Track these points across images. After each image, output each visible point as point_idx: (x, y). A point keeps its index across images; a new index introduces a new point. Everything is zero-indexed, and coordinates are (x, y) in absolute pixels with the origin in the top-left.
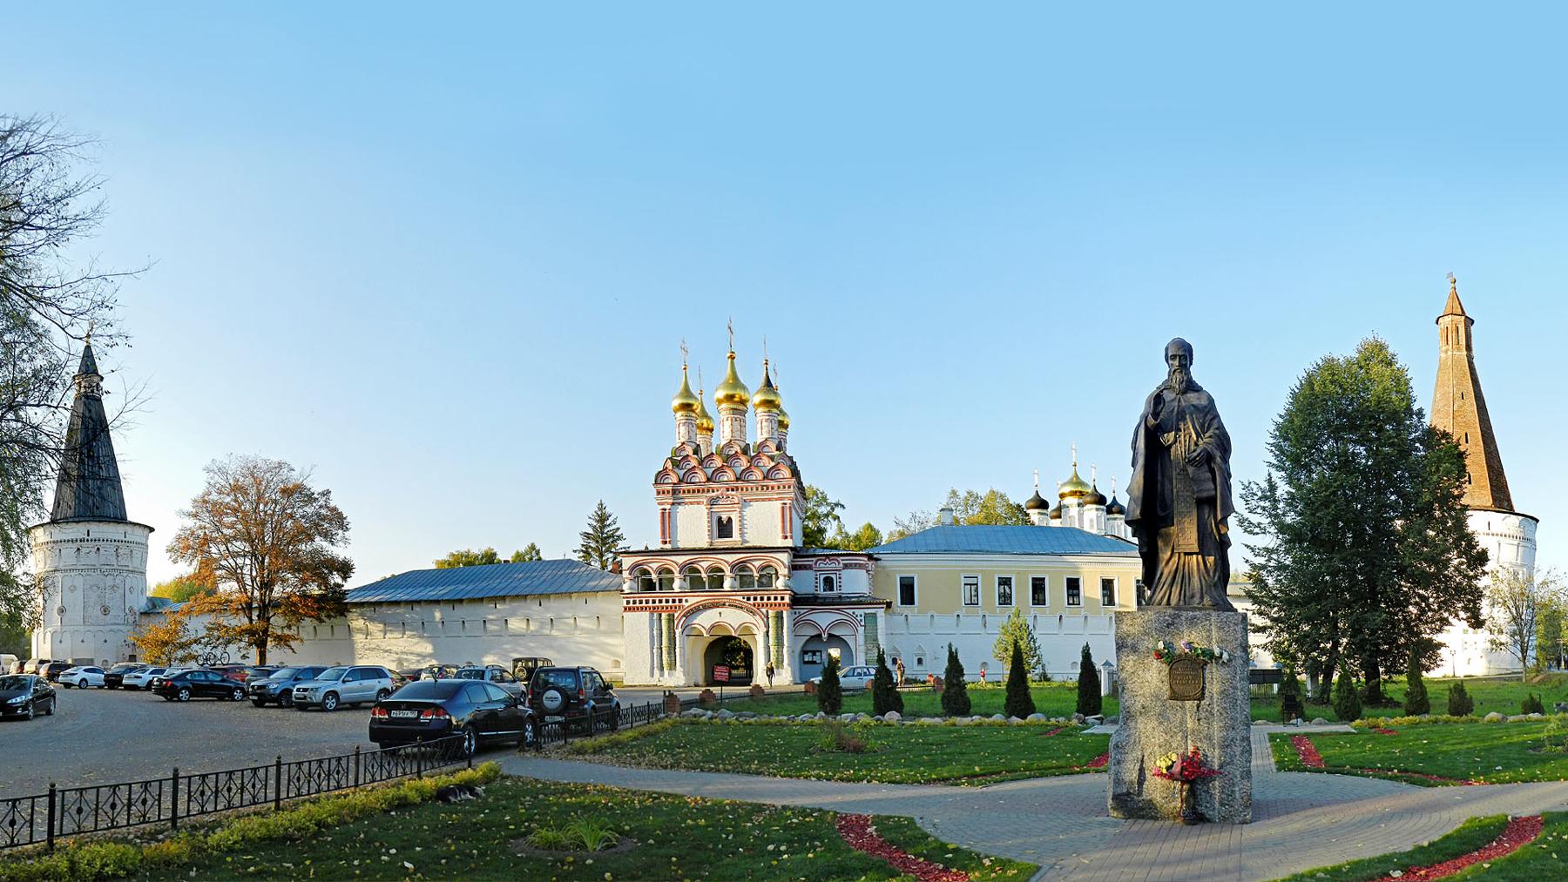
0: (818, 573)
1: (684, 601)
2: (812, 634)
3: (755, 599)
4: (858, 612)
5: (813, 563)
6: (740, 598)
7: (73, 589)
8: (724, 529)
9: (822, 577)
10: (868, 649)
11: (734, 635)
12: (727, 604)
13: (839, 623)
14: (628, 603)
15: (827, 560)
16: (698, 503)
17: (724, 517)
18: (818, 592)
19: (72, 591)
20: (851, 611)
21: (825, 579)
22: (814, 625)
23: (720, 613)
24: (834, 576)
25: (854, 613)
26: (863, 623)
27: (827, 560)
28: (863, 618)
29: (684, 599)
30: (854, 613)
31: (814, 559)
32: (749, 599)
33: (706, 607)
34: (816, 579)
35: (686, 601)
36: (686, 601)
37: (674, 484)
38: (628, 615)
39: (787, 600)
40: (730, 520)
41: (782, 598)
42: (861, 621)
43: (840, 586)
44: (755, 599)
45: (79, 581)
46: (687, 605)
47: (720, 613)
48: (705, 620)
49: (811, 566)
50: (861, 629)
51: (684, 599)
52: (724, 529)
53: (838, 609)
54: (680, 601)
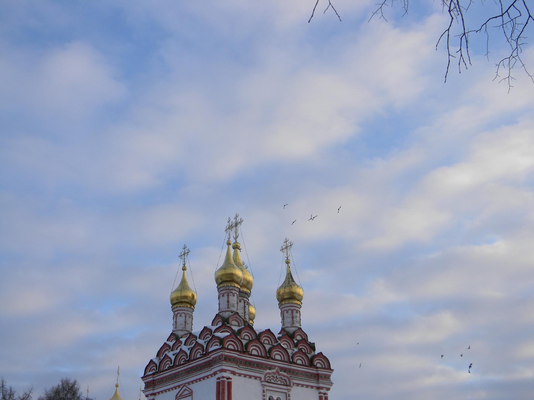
16: (256, 378)
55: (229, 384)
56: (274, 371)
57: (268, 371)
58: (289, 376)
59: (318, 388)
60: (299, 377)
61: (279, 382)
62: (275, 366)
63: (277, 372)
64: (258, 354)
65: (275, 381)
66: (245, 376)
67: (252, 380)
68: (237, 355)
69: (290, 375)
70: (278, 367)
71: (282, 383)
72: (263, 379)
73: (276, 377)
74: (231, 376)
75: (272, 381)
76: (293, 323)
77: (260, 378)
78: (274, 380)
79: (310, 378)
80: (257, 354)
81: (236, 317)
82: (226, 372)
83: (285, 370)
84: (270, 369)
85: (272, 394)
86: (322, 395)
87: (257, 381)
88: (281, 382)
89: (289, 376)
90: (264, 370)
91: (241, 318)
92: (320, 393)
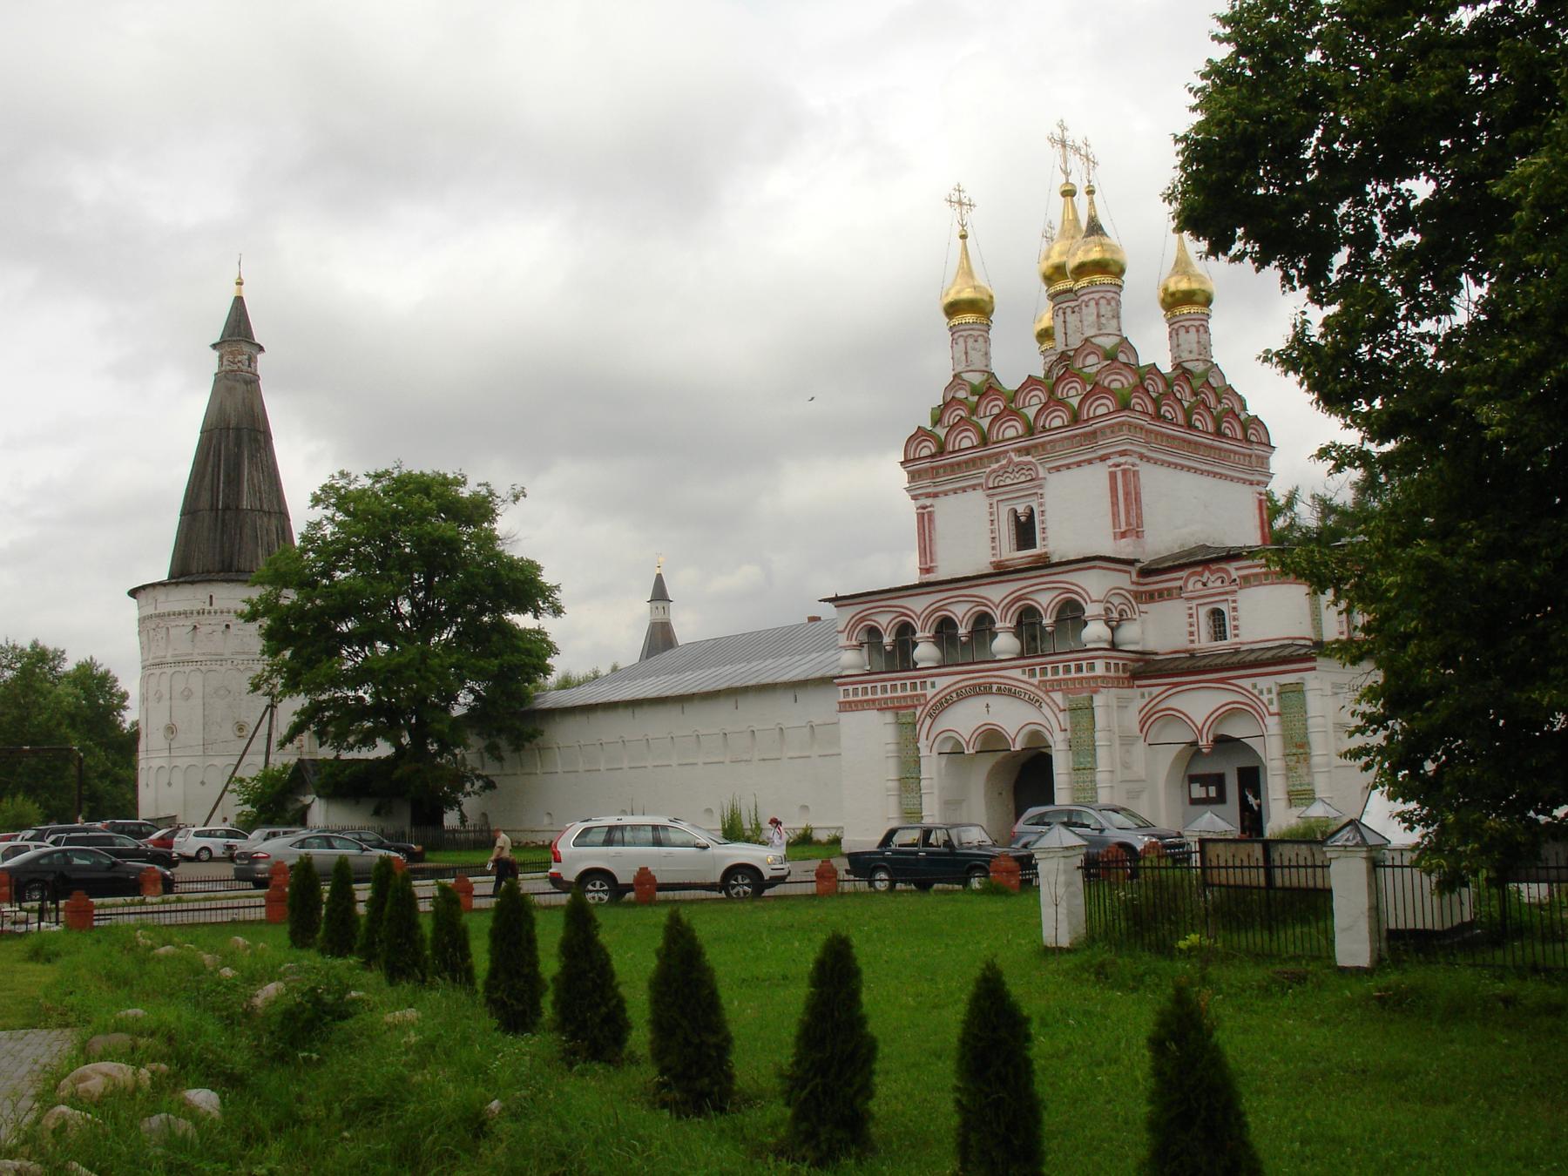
0: (1195, 603)
1: (928, 684)
3: (1044, 672)
4: (1264, 683)
6: (1017, 673)
7: (188, 695)
8: (1025, 531)
9: (1203, 611)
10: (1288, 768)
12: (995, 687)
13: (1232, 713)
15: (1207, 574)
16: (974, 487)
17: (1021, 509)
18: (1196, 645)
19: (187, 698)
20: (1246, 683)
22: (1176, 717)
23: (987, 706)
24: (1223, 607)
25: (1255, 686)
28: (1274, 696)
30: (1255, 686)
33: (962, 695)
34: (1191, 616)
36: (933, 685)
41: (1092, 667)
44: (1044, 672)
45: (196, 682)
46: (930, 692)
47: (987, 706)
48: (966, 720)
51: (929, 680)
52: (1025, 531)
55: (930, 514)
56: (1004, 462)
59: (1103, 459)
61: (1023, 479)
62: (1007, 452)
66: (955, 491)
67: (971, 494)
70: (1013, 450)
71: (1029, 478)
74: (928, 502)
75: (1009, 481)
77: (980, 485)
80: (970, 445)
83: (1027, 451)
84: (997, 461)
87: (980, 493)
89: (1033, 460)
92: (1110, 467)
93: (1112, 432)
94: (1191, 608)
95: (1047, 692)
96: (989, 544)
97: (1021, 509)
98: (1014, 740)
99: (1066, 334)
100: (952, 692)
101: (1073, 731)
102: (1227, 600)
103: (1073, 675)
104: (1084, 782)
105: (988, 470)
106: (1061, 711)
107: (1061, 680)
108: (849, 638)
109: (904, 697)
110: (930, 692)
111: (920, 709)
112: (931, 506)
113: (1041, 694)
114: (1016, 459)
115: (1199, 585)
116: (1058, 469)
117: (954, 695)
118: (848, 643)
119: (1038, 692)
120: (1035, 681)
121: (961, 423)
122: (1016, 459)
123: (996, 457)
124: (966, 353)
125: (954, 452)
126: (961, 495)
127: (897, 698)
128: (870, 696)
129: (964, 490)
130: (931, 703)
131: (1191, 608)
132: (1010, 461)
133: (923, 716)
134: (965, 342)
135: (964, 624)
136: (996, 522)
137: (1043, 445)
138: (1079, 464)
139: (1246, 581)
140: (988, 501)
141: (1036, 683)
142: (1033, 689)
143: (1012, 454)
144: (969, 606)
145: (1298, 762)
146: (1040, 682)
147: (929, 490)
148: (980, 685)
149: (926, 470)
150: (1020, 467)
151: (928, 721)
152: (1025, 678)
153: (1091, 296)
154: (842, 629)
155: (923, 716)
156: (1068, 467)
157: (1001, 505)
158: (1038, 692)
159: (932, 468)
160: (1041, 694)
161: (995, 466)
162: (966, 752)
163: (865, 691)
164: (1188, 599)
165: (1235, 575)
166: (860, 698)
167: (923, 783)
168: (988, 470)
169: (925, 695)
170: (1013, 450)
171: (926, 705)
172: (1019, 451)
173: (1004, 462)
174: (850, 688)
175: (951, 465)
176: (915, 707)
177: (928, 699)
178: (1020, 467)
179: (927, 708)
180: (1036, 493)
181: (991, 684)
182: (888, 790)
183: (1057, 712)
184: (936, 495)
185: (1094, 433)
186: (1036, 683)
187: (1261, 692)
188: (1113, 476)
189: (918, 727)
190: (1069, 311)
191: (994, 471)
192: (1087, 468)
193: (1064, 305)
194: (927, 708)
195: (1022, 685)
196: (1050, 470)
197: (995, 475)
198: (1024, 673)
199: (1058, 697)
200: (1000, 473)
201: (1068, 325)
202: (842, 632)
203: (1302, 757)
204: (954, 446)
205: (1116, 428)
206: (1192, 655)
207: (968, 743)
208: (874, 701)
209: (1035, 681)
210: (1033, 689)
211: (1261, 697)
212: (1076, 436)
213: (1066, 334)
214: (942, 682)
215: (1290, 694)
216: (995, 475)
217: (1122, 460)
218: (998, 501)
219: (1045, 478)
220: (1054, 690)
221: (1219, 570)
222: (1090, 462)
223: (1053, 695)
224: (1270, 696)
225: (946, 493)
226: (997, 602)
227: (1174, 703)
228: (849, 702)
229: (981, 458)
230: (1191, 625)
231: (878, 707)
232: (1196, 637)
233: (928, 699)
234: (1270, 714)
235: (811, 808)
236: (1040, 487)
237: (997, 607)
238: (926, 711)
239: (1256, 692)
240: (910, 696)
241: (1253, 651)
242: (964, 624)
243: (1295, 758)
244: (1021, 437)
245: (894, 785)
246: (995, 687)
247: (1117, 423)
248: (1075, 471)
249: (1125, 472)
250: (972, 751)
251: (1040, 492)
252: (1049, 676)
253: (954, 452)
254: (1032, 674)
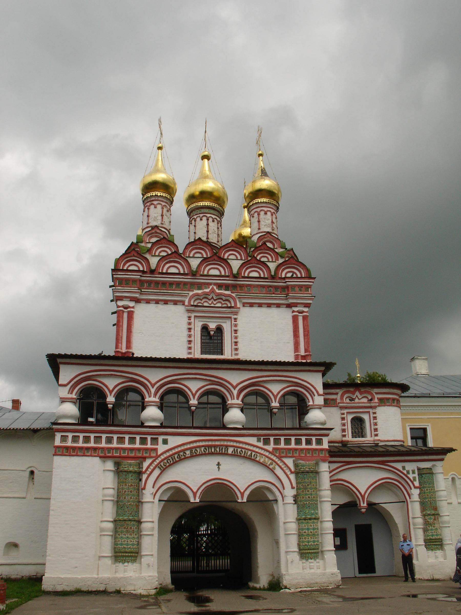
0: (345, 411)
2: (341, 503)
3: (277, 441)
4: (410, 467)
5: (338, 397)
9: (350, 417)
10: (426, 523)
11: (240, 501)
12: (230, 450)
14: (64, 438)
16: (175, 303)
17: (212, 326)
20: (399, 466)
21: (353, 420)
23: (219, 464)
24: (366, 417)
26: (417, 484)
27: (357, 393)
28: (416, 475)
29: (161, 438)
30: (404, 468)
31: (340, 392)
32: (267, 442)
34: (343, 419)
35: (165, 442)
36: (165, 442)
37: (143, 272)
38: (59, 461)
39: (325, 445)
40: (219, 330)
41: (319, 442)
42: (414, 478)
43: (376, 430)
44: (277, 441)
46: (161, 448)
47: (219, 464)
49: (335, 400)
50: (415, 493)
51: (161, 438)
53: (383, 463)
54: (154, 441)
56: (207, 290)
57: (196, 292)
58: (234, 295)
59: (289, 306)
60: (253, 293)
61: (219, 305)
62: (210, 284)
63: (213, 291)
64: (179, 271)
65: (210, 304)
66: (157, 302)
67: (171, 307)
68: (139, 277)
69: (236, 294)
70: (215, 284)
71: (225, 306)
72: (186, 303)
73: (212, 298)
74: (132, 304)
75: (206, 304)
76: (259, 229)
78: (208, 303)
79: (274, 294)
80: (177, 271)
81: (156, 233)
82: (140, 302)
83: (227, 287)
84: (199, 289)
85: (207, 321)
86: (297, 314)
87: (180, 309)
88: (222, 304)
89: (234, 295)
90: (189, 290)
91: (162, 233)
92: (293, 312)
93: (300, 290)
94: (343, 414)
95: (280, 458)
96: (186, 345)
97: (212, 326)
98: (242, 494)
99: (208, 232)
100: (187, 449)
101: (298, 489)
102: (369, 412)
103: (304, 446)
104: (308, 529)
105: (191, 293)
106: (292, 472)
107: (282, 449)
108: (71, 391)
109: (132, 450)
110: (161, 448)
111: (148, 462)
112: (133, 307)
113: (274, 458)
114: (218, 291)
115: (348, 401)
116: (251, 305)
117: (188, 452)
118: (70, 396)
119: (272, 457)
120: (270, 447)
121: (173, 255)
122: (218, 291)
123: (200, 286)
124: (162, 216)
125: (163, 273)
126: (161, 307)
127: (124, 449)
128: (92, 444)
129: (166, 302)
130: (162, 457)
131: (343, 414)
132: (213, 291)
133: (152, 467)
134: (163, 208)
135: (196, 397)
136: (192, 330)
137: (242, 286)
138: (269, 305)
139: (383, 402)
140: (187, 315)
141: (271, 449)
142: (267, 454)
143: (215, 288)
144: (201, 384)
145: (435, 519)
146: (274, 449)
147: (137, 295)
148: (215, 446)
149: (134, 281)
150: (219, 297)
151: (157, 472)
152: (261, 444)
153: (269, 209)
154: (65, 382)
155: (152, 467)
156: (260, 305)
157: (197, 320)
158: (272, 457)
159: (140, 281)
160: (274, 458)
161: (200, 292)
162: (192, 500)
163: (75, 439)
164: (342, 408)
165: (376, 396)
166: (80, 444)
167: (144, 525)
168: (191, 293)
169: (156, 450)
170: (215, 284)
171: (157, 457)
172: (220, 286)
173: (207, 290)
174: (70, 435)
175: (157, 283)
176: (144, 458)
177: (159, 453)
178: (219, 297)
179: (158, 461)
180: (230, 318)
181: (227, 446)
182: (102, 530)
183: (289, 473)
184: (138, 301)
185: (287, 287)
186: (271, 449)
187: (408, 472)
188: (295, 319)
189: (144, 477)
190: (211, 220)
191: (197, 295)
192: (274, 311)
193: (208, 215)
194: (158, 461)
195: (257, 450)
196: (244, 305)
197: (196, 297)
198: (259, 440)
199: (290, 462)
200: (201, 297)
201: (209, 227)
202: (65, 385)
203: (436, 516)
204: (162, 270)
205: (303, 289)
206: (344, 444)
207: (195, 494)
208: (95, 449)
209: (270, 447)
210: (267, 454)
211: (408, 475)
212: (270, 286)
213: (208, 232)
214: (174, 441)
215: (428, 475)
216: (196, 297)
217: (306, 309)
218: (195, 316)
219: (239, 308)
220: (286, 457)
221: (365, 392)
222: (278, 306)
223: (286, 460)
224: (414, 475)
225: (148, 302)
226: (235, 384)
227: (343, 476)
228: (67, 448)
229: (185, 284)
230: (344, 425)
231: (102, 455)
232: (346, 433)
233: (159, 453)
234: (415, 487)
235: (20, 545)
236: (236, 313)
237: (235, 388)
238: (155, 463)
239: (405, 472)
240: (139, 449)
241: (392, 446)
242: (196, 397)
243: (433, 517)
244: (228, 276)
245: (111, 525)
246: (230, 450)
247: (305, 285)
248: (264, 310)
249: (305, 318)
250: (198, 500)
251: (233, 317)
252: (282, 445)
253: (163, 273)
254: (267, 442)
